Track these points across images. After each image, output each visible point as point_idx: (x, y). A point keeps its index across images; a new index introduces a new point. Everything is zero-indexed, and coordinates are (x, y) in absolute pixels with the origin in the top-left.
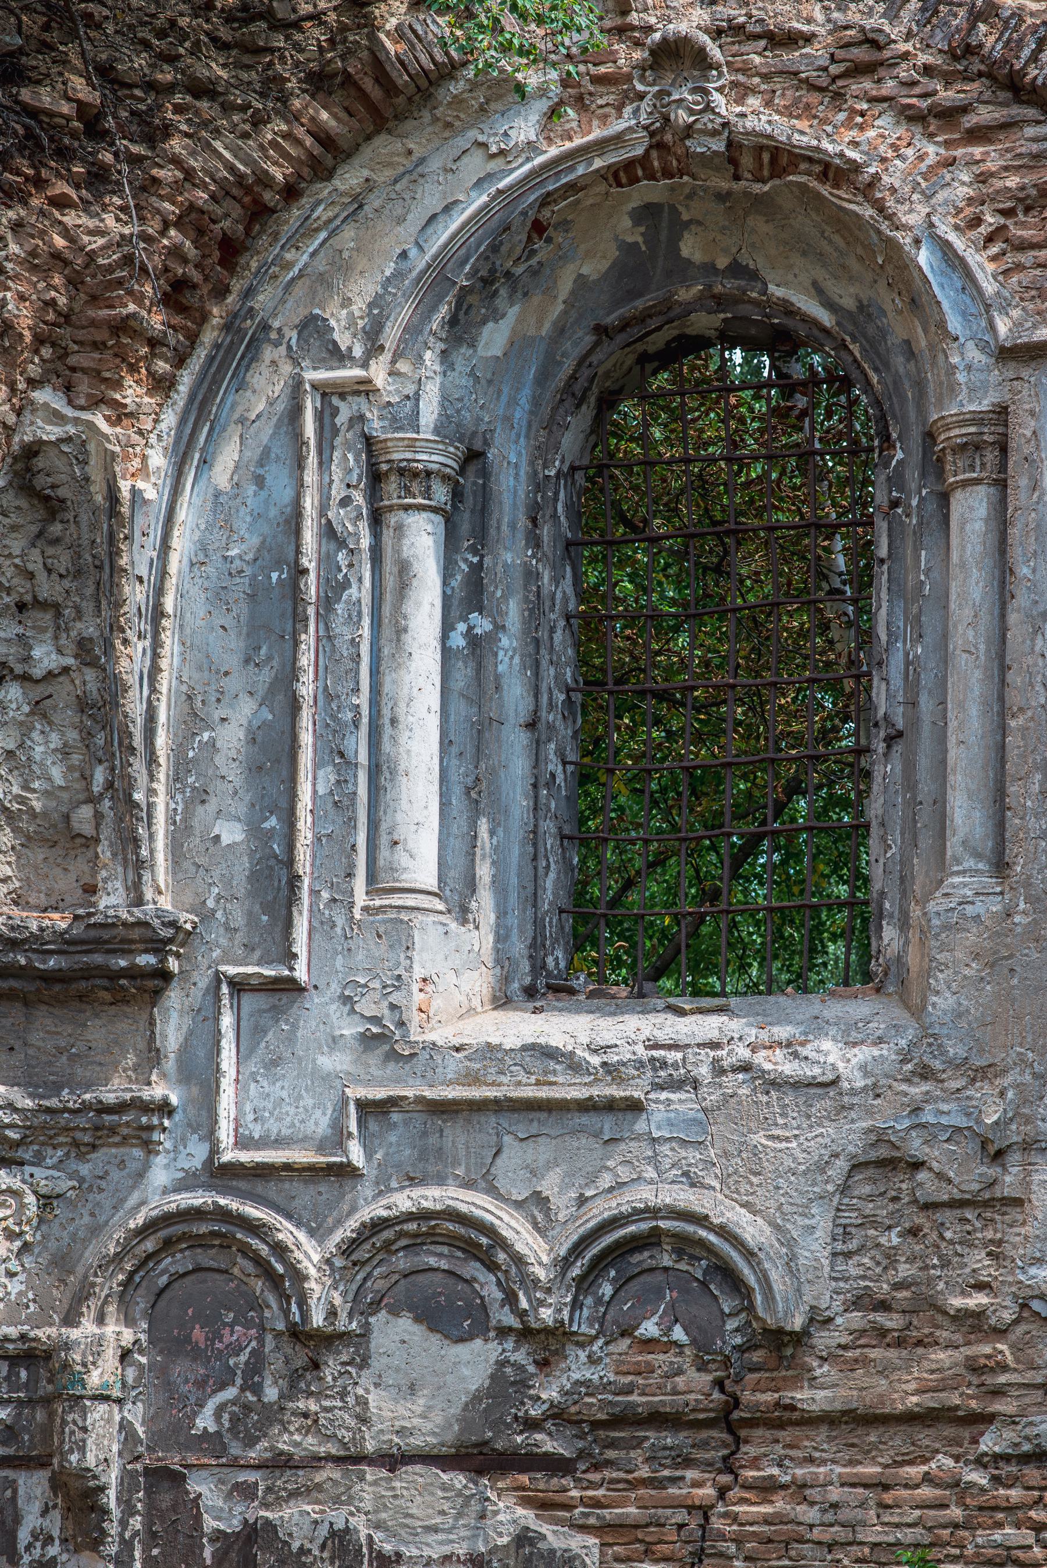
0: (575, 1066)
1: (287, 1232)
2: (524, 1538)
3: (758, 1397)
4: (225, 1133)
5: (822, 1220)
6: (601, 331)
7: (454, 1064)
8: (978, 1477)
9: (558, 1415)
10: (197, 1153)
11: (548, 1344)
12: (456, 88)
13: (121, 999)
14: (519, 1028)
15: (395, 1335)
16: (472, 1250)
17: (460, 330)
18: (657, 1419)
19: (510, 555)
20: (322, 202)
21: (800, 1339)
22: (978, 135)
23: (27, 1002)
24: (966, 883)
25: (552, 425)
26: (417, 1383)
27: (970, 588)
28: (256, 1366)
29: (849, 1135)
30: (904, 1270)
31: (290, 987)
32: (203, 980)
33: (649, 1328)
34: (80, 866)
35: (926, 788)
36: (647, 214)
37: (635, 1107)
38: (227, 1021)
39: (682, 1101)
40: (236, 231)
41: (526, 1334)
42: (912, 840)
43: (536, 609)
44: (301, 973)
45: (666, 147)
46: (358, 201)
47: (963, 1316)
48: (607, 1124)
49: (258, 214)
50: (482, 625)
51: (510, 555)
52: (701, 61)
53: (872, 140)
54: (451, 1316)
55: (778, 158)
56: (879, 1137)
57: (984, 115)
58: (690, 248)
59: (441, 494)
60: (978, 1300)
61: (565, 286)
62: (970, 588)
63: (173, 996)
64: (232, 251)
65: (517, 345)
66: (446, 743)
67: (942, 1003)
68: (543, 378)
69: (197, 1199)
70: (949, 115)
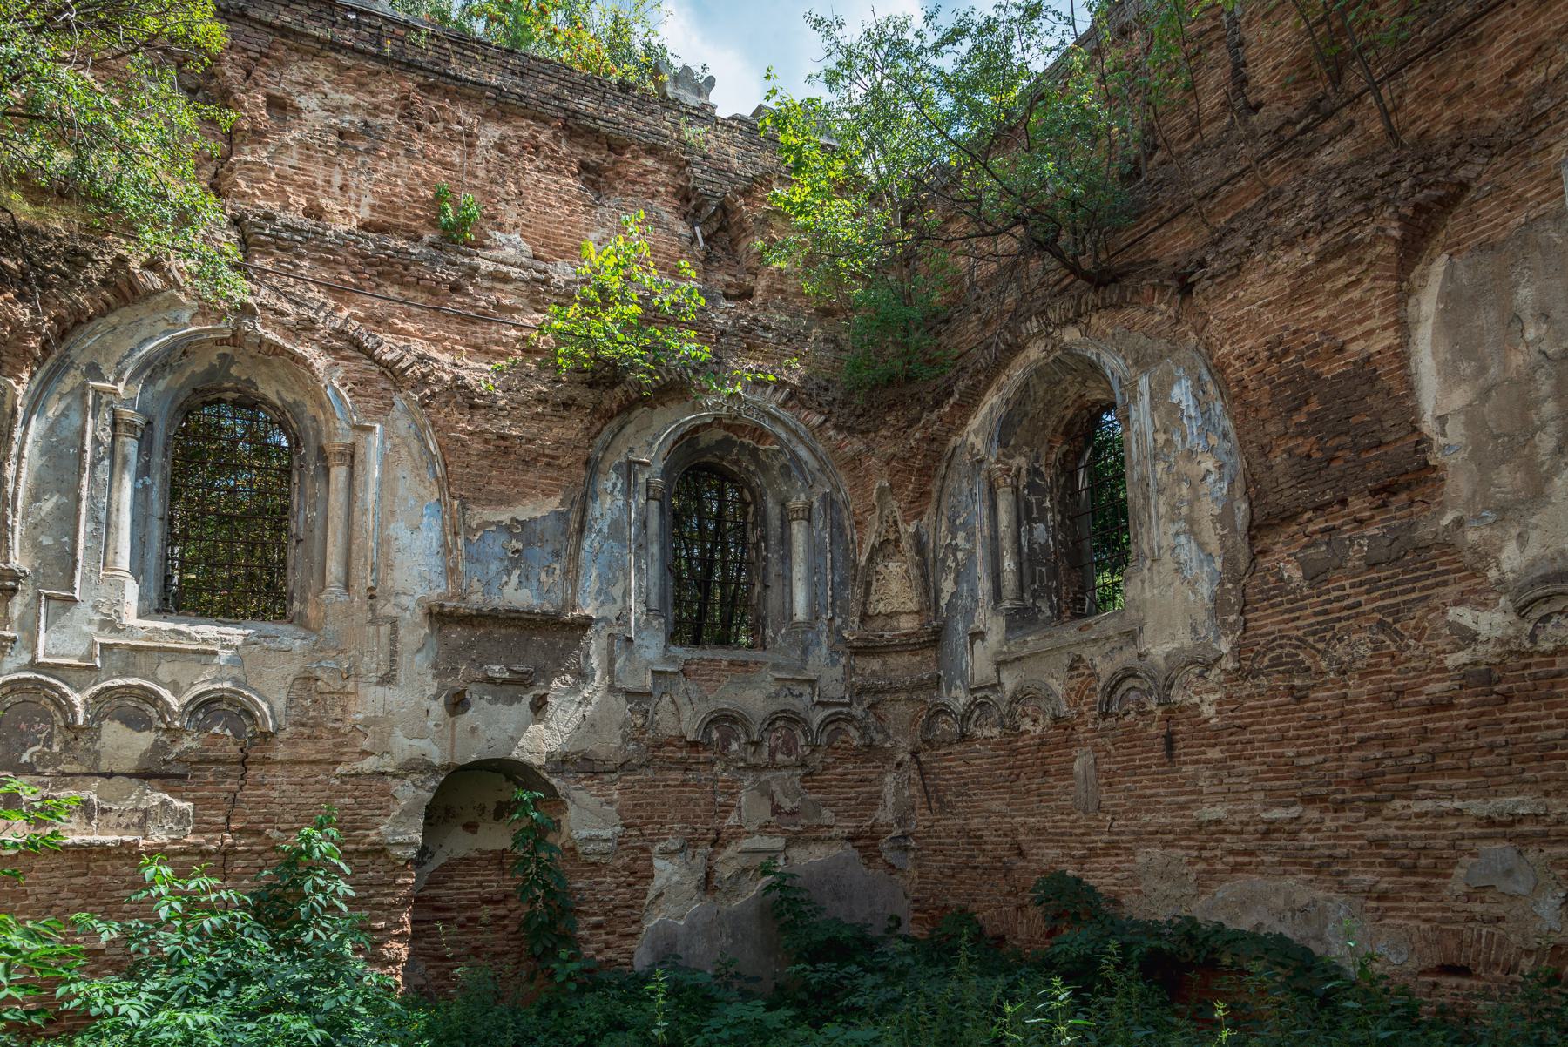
2: (164, 803)
4: (40, 651)
5: (284, 693)
9: (178, 759)
10: (26, 658)
11: (175, 734)
12: (159, 299)
17: (151, 380)
18: (217, 761)
20: (101, 325)
21: (272, 735)
22: (344, 358)
27: (337, 499)
28: (50, 738)
29: (295, 668)
30: (311, 714)
31: (74, 600)
33: (217, 730)
37: (215, 653)
38: (43, 610)
44: (77, 596)
48: (203, 658)
49: (78, 323)
50: (149, 482)
51: (157, 460)
52: (253, 314)
54: (136, 722)
55: (277, 350)
57: (349, 353)
58: (234, 371)
59: (139, 434)
60: (337, 725)
61: (187, 373)
63: (18, 598)
65: (167, 389)
68: (173, 401)
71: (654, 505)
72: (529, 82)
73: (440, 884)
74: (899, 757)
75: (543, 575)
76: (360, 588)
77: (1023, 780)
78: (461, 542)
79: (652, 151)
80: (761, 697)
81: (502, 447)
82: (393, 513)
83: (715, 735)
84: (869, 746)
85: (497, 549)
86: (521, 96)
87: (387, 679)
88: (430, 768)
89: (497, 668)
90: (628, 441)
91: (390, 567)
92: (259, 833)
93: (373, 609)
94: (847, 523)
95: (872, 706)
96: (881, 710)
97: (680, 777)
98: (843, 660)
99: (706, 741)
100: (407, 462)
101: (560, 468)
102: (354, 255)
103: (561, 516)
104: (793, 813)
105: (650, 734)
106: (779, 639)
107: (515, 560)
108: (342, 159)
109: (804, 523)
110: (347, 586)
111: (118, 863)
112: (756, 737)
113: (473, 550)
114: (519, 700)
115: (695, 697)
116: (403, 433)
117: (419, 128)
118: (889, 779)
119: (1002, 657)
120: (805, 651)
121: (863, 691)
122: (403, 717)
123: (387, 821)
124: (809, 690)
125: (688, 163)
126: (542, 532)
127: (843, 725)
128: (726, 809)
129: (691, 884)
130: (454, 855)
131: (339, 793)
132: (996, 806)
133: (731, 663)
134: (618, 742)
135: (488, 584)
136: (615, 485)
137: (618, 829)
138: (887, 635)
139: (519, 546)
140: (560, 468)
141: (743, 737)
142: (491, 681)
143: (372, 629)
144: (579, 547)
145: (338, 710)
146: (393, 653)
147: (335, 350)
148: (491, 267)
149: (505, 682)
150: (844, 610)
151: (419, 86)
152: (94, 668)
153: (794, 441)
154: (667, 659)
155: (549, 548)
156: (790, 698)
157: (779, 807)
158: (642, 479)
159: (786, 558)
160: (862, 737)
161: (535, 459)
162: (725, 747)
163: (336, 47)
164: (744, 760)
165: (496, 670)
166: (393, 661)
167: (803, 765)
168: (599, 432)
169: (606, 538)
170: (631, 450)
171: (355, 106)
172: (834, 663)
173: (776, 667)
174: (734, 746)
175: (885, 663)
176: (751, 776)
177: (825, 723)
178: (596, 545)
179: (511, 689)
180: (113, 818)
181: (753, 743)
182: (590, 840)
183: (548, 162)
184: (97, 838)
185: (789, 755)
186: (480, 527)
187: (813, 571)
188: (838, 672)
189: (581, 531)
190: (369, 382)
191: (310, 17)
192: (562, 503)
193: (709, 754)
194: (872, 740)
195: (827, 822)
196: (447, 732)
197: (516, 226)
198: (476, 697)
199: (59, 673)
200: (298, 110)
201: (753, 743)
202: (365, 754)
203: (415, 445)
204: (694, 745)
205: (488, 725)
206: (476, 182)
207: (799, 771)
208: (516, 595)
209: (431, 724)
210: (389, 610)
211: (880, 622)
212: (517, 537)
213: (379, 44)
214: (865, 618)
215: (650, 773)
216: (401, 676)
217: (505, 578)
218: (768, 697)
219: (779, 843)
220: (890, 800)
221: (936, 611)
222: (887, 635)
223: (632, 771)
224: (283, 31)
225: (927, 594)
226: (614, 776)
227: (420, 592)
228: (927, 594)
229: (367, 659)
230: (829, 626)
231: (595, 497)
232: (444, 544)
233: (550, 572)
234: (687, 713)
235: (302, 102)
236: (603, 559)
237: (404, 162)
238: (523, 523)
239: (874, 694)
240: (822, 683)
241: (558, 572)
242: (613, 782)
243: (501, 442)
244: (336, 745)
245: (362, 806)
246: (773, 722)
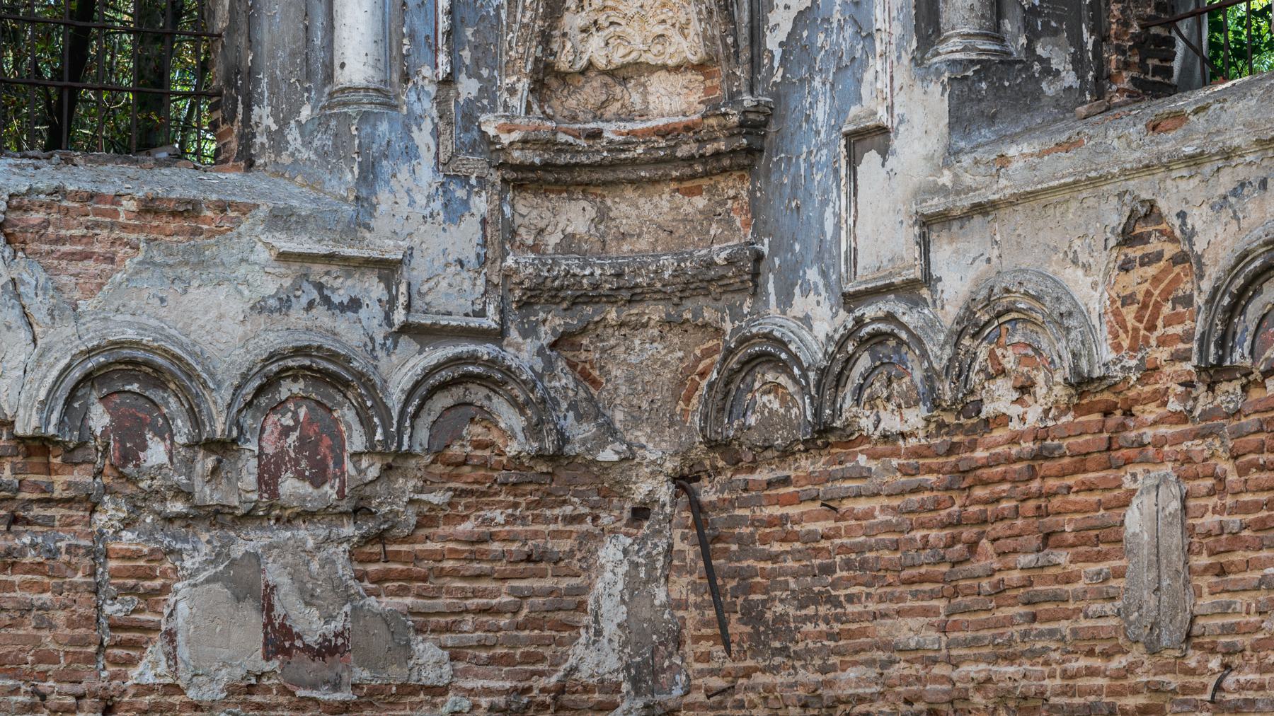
74: (641, 490)
77: (987, 557)
83: (99, 419)
84: (556, 458)
95: (563, 341)
96: (589, 351)
98: (481, 204)
99: (72, 438)
104: (327, 650)
106: (293, 135)
112: (219, 427)
115: (39, 307)
118: (609, 552)
119: (935, 204)
120: (369, 175)
121: (537, 295)
124: (373, 288)
127: (478, 394)
128: (131, 636)
132: (909, 631)
133: (149, 208)
138: (611, 131)
141: (182, 427)
150: (487, 55)
156: (322, 316)
157: (287, 631)
160: (534, 430)
162: (128, 456)
164: (184, 493)
167: (360, 511)
172: (454, 212)
173: (281, 219)
174: (156, 453)
175: (603, 216)
176: (205, 541)
177: (425, 389)
181: (211, 445)
188: (464, 238)
193: (81, 476)
194: (563, 439)
195: (429, 676)
201: (211, 445)
204: (37, 448)
207: (348, 530)
211: (591, 92)
214: (546, 78)
218: (259, 308)
220: (613, 614)
221: (754, 63)
222: (611, 131)
225: (730, 19)
228: (730, 19)
230: (441, 102)
239: (572, 304)
240: (418, 271)
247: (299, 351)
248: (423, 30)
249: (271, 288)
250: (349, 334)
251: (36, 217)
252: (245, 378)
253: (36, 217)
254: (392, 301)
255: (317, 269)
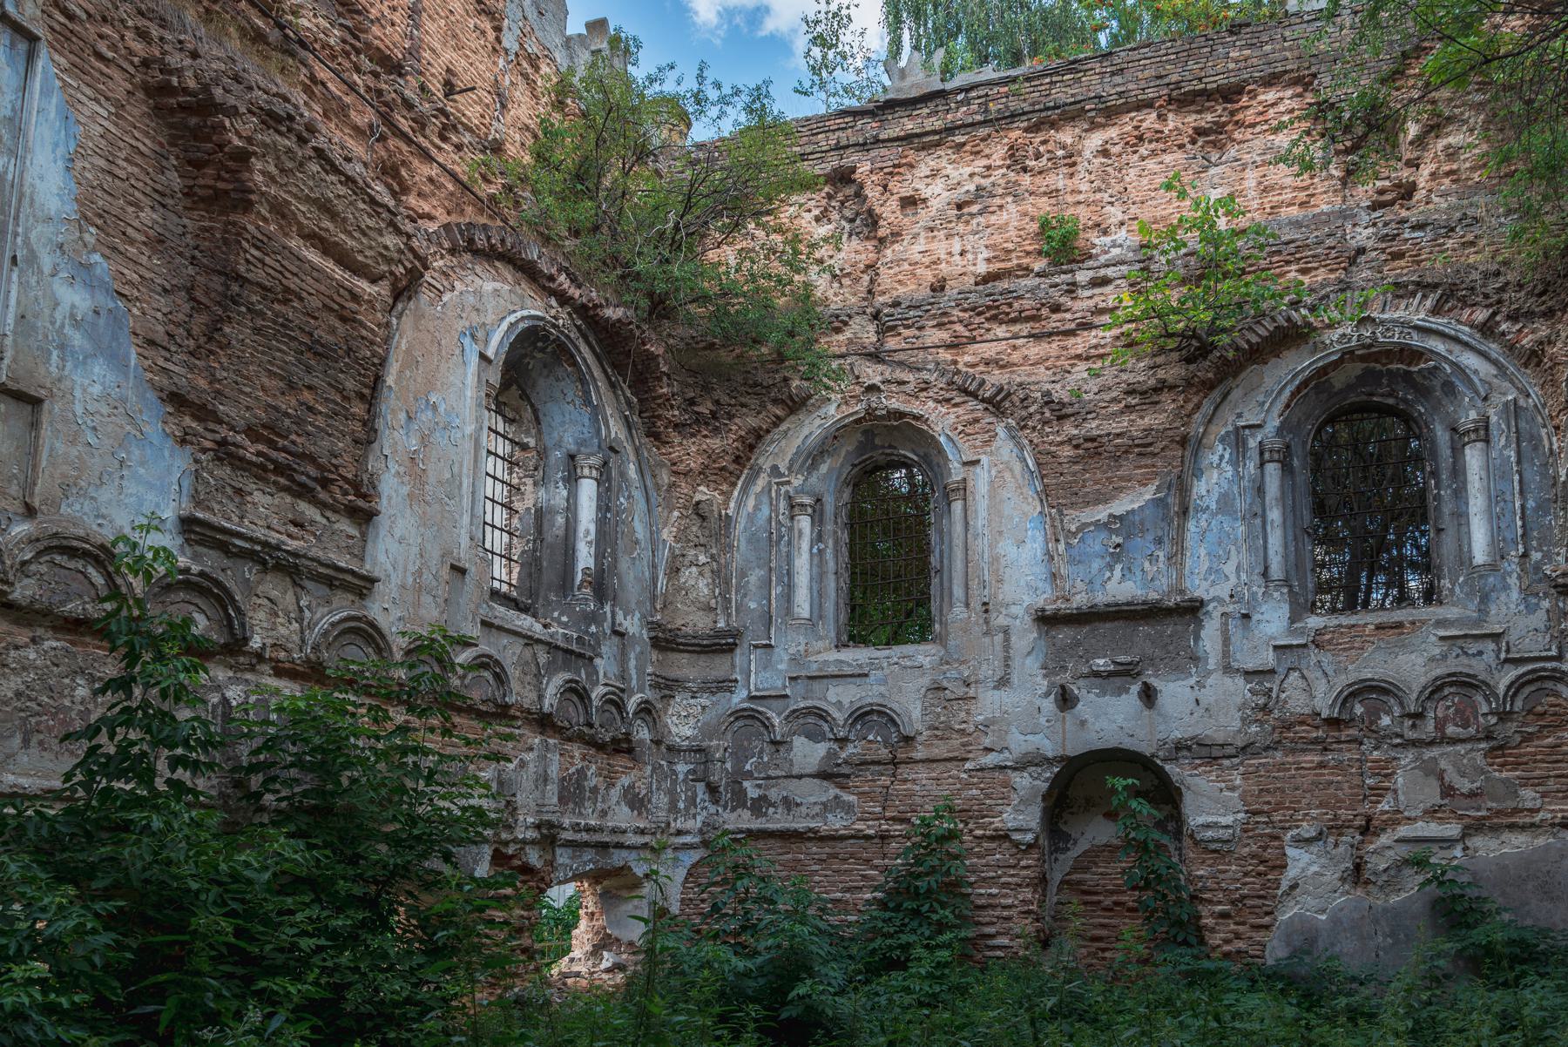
0: (849, 665)
1: (770, 714)
2: (836, 797)
3: (901, 756)
6: (854, 466)
7: (815, 666)
8: (964, 776)
9: (846, 762)
10: (744, 694)
13: (723, 651)
14: (833, 656)
15: (799, 742)
16: (821, 717)
17: (814, 466)
18: (874, 763)
19: (829, 527)
20: (776, 434)
21: (913, 739)
22: (956, 405)
23: (699, 653)
24: (959, 611)
25: (841, 491)
26: (808, 753)
27: (958, 528)
28: (761, 752)
29: (926, 681)
31: (770, 646)
32: (746, 646)
33: (871, 737)
34: (712, 615)
35: (946, 584)
36: (865, 432)
37: (866, 675)
39: (879, 673)
40: (754, 441)
41: (836, 740)
42: (942, 599)
43: (836, 542)
45: (870, 412)
46: (786, 432)
47: (958, 731)
48: (858, 680)
49: (759, 437)
50: (822, 546)
51: (829, 527)
52: (878, 389)
53: (926, 407)
54: (814, 736)
56: (935, 682)
57: (958, 400)
59: (810, 510)
60: (963, 726)
62: (958, 528)
63: (738, 651)
64: (752, 448)
66: (811, 579)
67: (952, 643)
69: (745, 705)
70: (948, 400)
71: (1272, 470)
72: (1128, 75)
73: (1086, 870)
75: (1147, 564)
76: (976, 604)
78: (1061, 547)
79: (1270, 81)
80: (1420, 661)
81: (1091, 449)
82: (1000, 533)
85: (1098, 547)
86: (1120, 94)
87: (1003, 682)
88: (1049, 761)
89: (1101, 662)
90: (1236, 406)
91: (1000, 581)
92: (908, 821)
93: (987, 622)
94: (1543, 432)
97: (1317, 759)
100: (1011, 484)
101: (1155, 455)
102: (965, 310)
103: (1159, 503)
105: (1276, 714)
107: (1117, 554)
108: (961, 228)
109: (1479, 445)
110: (967, 605)
111: (809, 845)
113: (1074, 552)
114: (1127, 691)
115: (1330, 670)
116: (1006, 458)
117: (1025, 170)
122: (1020, 714)
123: (1009, 809)
125: (1314, 76)
126: (1142, 523)
129: (1332, 876)
130: (1096, 842)
131: (968, 785)
133: (1379, 627)
134: (1237, 724)
135: (1091, 582)
136: (1222, 457)
137: (1241, 816)
139: (1119, 540)
140: (1155, 455)
142: (1097, 674)
143: (987, 640)
144: (1181, 529)
145: (963, 714)
146: (1007, 658)
147: (948, 400)
148: (1091, 274)
149: (1111, 674)
151: (1026, 130)
152: (786, 696)
153: (1457, 348)
154: (1292, 632)
155: (1150, 537)
156: (1465, 660)
158: (1252, 443)
159: (1460, 493)
161: (1126, 452)
163: (950, 130)
165: (1100, 663)
166: (1007, 666)
168: (1198, 407)
169: (1214, 515)
170: (1240, 416)
171: (971, 175)
173: (1440, 623)
178: (1203, 524)
179: (1118, 681)
180: (803, 809)
182: (1208, 826)
183: (1153, 146)
184: (795, 826)
185: (1465, 726)
186: (1079, 529)
187: (1495, 499)
189: (1184, 512)
190: (976, 421)
191: (929, 115)
192: (1158, 489)
196: (1059, 724)
197: (1122, 224)
198: (1084, 691)
199: (765, 702)
200: (924, 200)
202: (988, 750)
203: (1017, 467)
205: (1097, 717)
206: (1081, 197)
208: (1121, 588)
209: (1043, 720)
210: (1002, 621)
212: (1117, 532)
213: (986, 111)
215: (1279, 755)
216: (1015, 679)
217: (1108, 574)
218: (1432, 659)
219: (1453, 830)
223: (1256, 755)
224: (907, 138)
226: (1236, 761)
227: (1027, 600)
229: (984, 667)
231: (1198, 473)
232: (1048, 553)
233: (1152, 558)
234: (1321, 687)
235: (926, 192)
236: (1211, 537)
237: (1012, 208)
238: (1121, 518)
241: (1162, 558)
242: (1234, 767)
243: (1089, 445)
244: (964, 745)
245: (987, 796)
246: (1439, 689)
247: (1449, 675)
248: (1509, 536)
249: (1437, 651)
250: (1477, 667)
251: (1327, 637)
252: (1425, 688)
253: (1327, 637)
254: (1499, 650)
255: (1460, 642)
